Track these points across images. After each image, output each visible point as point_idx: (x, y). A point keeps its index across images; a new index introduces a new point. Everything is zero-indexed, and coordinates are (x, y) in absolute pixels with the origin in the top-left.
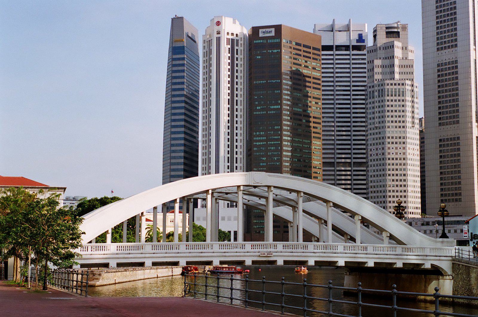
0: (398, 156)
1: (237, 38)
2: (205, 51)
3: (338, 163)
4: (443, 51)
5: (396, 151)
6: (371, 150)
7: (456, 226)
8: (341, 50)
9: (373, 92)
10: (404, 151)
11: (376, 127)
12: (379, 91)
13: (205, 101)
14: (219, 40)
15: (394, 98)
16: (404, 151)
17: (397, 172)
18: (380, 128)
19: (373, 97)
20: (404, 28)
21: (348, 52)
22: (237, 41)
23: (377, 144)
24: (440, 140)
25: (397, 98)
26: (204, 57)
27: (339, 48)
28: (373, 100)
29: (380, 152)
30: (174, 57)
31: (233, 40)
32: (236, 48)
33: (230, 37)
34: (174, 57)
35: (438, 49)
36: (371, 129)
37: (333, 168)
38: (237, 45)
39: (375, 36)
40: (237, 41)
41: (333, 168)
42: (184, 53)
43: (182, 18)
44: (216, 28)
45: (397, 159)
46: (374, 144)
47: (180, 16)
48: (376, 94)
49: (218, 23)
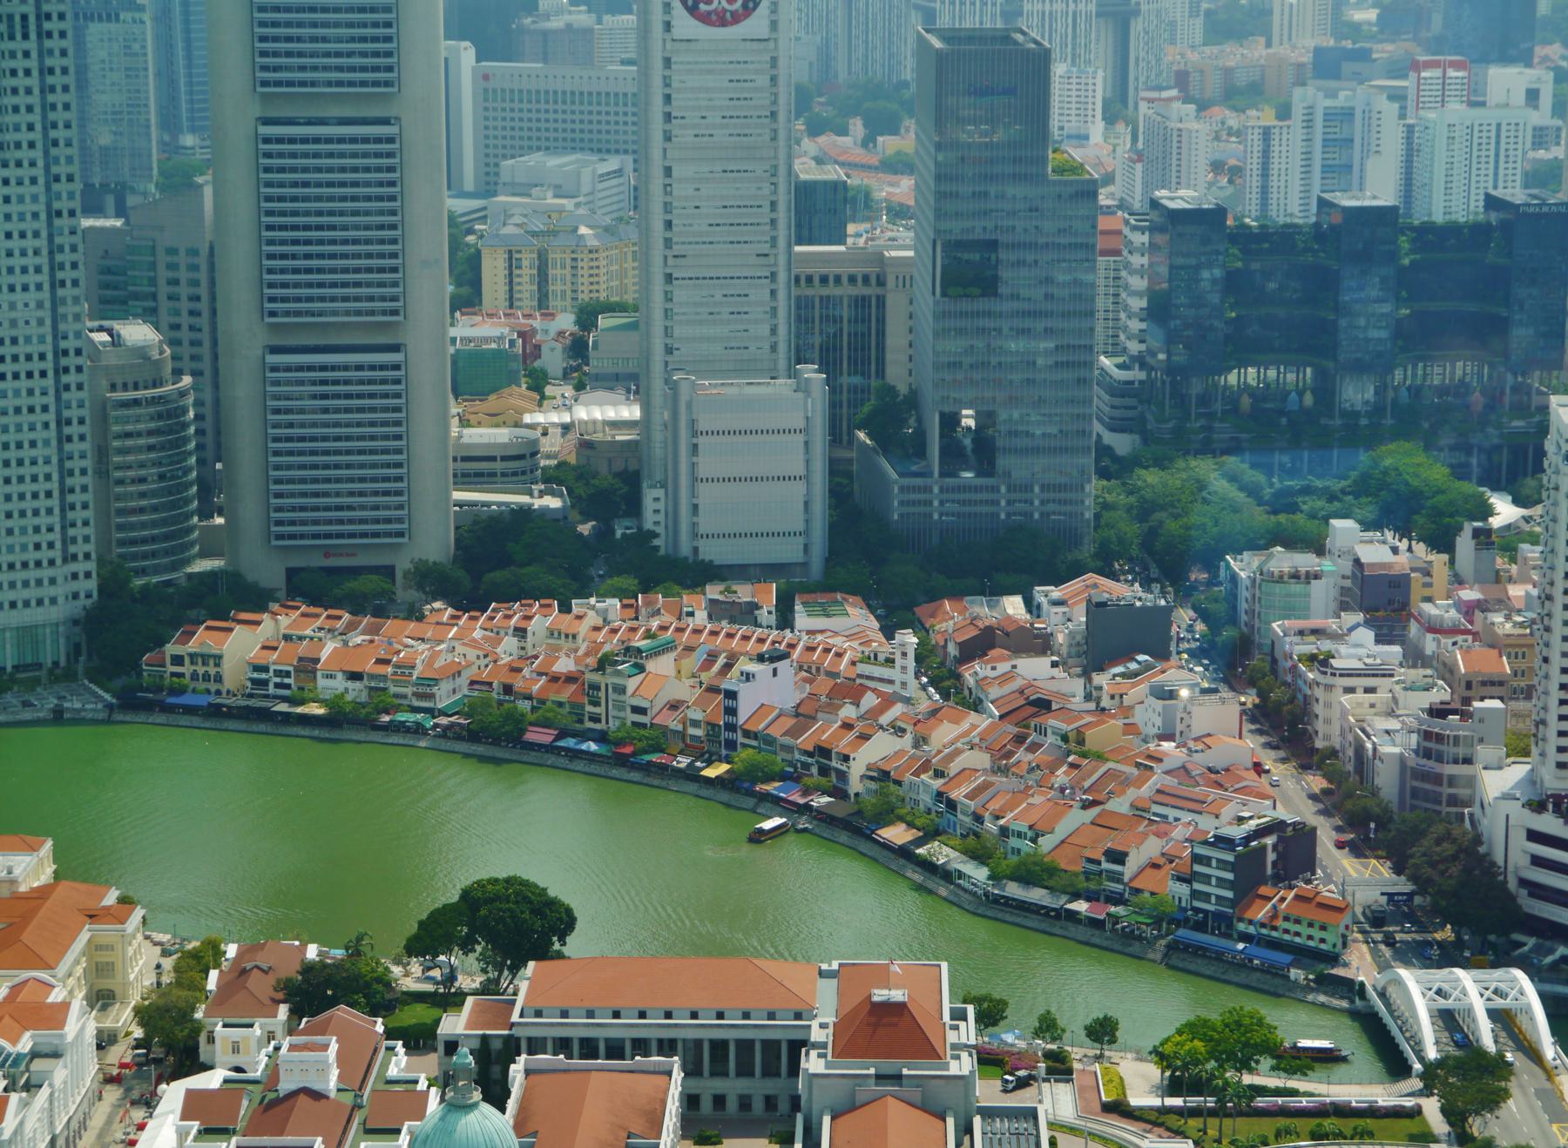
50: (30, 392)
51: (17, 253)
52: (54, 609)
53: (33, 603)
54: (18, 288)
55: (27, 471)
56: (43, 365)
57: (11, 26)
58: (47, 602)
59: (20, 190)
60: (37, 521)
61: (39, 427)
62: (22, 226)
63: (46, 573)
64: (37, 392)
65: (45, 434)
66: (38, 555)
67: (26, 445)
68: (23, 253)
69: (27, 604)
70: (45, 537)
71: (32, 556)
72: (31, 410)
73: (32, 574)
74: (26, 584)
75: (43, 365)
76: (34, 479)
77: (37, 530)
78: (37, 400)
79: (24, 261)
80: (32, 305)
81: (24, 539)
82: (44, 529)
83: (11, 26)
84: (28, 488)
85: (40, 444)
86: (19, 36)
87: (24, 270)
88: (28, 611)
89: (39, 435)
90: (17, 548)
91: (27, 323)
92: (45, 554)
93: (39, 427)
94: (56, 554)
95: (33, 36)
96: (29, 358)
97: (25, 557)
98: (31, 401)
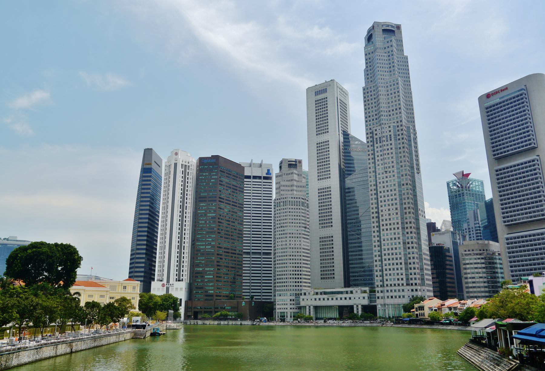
0: (296, 246)
1: (189, 165)
2: (166, 172)
3: (252, 252)
4: (322, 181)
5: (295, 243)
6: (278, 242)
7: (337, 295)
8: (256, 179)
9: (280, 202)
10: (300, 243)
11: (282, 227)
12: (284, 202)
13: (164, 206)
14: (176, 165)
15: (293, 207)
16: (300, 243)
17: (295, 258)
18: (284, 227)
19: (280, 206)
20: (300, 162)
21: (260, 181)
22: (189, 166)
23: (282, 238)
24: (320, 238)
25: (296, 207)
26: (165, 176)
27: (255, 177)
28: (280, 208)
29: (284, 243)
30: (144, 175)
31: (186, 166)
32: (187, 171)
33: (184, 163)
34: (144, 175)
35: (318, 179)
36: (278, 228)
37: (249, 256)
38: (189, 169)
39: (280, 167)
40: (189, 166)
41: (249, 256)
42: (151, 172)
43: (151, 149)
44: (175, 156)
45: (295, 248)
46: (280, 238)
47: (150, 148)
48: (282, 204)
49: (176, 154)
50: (395, 234)
51: (390, 195)
52: (404, 299)
53: (398, 297)
54: (391, 205)
55: (394, 256)
56: (398, 226)
57: (387, 138)
58: (402, 297)
59: (390, 179)
60: (398, 272)
61: (397, 243)
62: (391, 188)
63: (401, 288)
64: (397, 233)
65: (399, 246)
66: (398, 282)
67: (394, 249)
68: (392, 195)
69: (396, 297)
70: (400, 277)
71: (397, 282)
72: (395, 239)
73: (397, 288)
74: (395, 291)
75: (398, 226)
76: (397, 259)
77: (398, 274)
78: (397, 236)
79: (392, 197)
80: (394, 209)
81: (394, 277)
82: (400, 274)
83: (387, 138)
84: (395, 261)
85: (398, 249)
86: (389, 140)
87: (392, 200)
88: (396, 299)
89: (398, 246)
90: (392, 280)
91: (393, 214)
92: (400, 282)
93: (397, 243)
94: (404, 282)
95: (393, 139)
96: (394, 224)
97: (395, 282)
98: (395, 236)
